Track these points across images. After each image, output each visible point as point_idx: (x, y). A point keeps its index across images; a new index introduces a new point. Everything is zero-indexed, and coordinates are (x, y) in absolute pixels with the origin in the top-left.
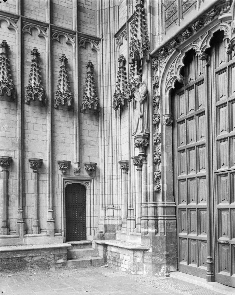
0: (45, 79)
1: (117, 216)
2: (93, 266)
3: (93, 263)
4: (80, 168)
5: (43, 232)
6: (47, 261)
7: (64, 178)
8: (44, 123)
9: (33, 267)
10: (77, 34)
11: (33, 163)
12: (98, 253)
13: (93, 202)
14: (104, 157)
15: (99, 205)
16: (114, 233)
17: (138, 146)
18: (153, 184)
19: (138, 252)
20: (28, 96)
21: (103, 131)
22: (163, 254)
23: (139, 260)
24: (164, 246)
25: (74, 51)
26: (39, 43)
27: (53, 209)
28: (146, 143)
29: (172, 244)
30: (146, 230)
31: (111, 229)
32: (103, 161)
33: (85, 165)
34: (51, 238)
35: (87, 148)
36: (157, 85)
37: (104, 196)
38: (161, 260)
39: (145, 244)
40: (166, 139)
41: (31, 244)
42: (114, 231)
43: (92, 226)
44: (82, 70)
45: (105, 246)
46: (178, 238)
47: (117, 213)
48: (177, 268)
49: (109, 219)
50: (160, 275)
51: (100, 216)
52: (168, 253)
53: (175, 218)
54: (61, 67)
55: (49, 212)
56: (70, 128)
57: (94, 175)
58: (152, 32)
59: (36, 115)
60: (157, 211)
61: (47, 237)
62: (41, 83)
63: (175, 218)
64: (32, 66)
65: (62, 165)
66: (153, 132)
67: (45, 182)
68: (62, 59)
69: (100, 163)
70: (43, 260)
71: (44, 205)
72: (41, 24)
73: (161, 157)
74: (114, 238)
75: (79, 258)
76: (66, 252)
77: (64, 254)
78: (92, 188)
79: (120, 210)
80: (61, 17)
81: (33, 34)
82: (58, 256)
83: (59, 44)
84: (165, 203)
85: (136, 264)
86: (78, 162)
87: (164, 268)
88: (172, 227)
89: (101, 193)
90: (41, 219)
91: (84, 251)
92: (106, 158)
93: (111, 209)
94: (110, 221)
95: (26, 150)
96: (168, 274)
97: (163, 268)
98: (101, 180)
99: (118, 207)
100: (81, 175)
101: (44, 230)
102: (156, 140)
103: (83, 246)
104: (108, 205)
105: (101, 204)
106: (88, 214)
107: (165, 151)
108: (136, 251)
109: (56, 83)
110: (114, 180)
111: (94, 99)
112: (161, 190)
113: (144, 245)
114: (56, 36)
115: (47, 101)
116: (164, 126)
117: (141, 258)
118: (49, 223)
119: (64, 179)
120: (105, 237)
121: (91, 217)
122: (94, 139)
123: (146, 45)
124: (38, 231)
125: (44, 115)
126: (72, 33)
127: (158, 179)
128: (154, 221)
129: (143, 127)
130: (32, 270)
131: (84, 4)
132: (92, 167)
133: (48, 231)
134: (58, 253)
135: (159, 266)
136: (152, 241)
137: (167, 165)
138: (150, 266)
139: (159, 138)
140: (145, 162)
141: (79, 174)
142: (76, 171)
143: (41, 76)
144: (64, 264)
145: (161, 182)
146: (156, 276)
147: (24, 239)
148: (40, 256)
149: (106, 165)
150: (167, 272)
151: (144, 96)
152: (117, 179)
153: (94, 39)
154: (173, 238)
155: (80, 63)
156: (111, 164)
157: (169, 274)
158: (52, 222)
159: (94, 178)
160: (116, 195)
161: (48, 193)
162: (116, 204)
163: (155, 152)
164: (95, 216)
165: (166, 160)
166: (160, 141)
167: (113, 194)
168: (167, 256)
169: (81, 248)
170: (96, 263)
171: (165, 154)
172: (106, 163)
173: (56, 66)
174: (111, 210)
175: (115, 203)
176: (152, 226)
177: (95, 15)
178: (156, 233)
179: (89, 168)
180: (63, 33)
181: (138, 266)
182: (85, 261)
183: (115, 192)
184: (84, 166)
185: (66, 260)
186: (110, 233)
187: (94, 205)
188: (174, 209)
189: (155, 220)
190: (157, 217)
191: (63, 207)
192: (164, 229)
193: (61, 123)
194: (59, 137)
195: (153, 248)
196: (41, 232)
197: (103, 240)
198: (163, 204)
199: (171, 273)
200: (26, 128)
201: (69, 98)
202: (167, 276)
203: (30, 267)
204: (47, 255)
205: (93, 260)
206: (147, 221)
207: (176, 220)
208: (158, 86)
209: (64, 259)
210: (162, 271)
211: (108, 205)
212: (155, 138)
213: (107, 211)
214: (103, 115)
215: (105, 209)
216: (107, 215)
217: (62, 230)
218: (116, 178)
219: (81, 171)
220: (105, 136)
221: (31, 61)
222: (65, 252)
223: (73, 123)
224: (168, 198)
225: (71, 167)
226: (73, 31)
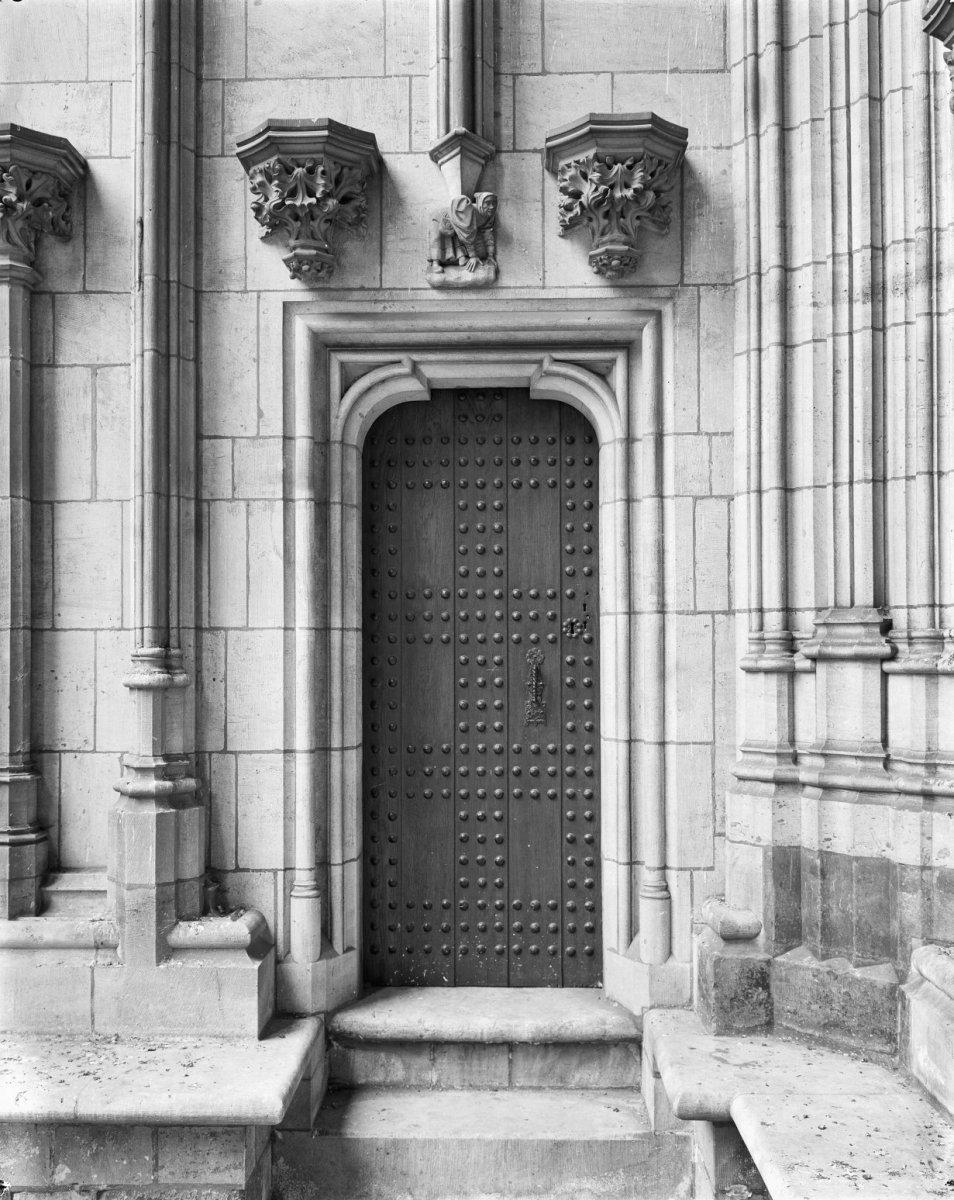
4: (494, 201)
5: (72, 903)
7: (320, 324)
14: (783, 47)
15: (730, 612)
16: (881, 975)
31: (847, 916)
37: (772, 500)
42: (887, 947)
43: (648, 854)
49: (828, 789)
51: (740, 741)
55: (133, 688)
57: (662, 276)
61: (81, 960)
69: (738, 135)
71: (107, 617)
78: (644, 427)
89: (741, 479)
90: (67, 758)
93: (853, 673)
94: (841, 810)
100: (505, 281)
103: (538, 1065)
104: (819, 610)
105: (743, 599)
110: (895, 306)
119: (324, 347)
120: (784, 1004)
121: (631, 742)
132: (617, 167)
141: (483, 273)
142: (448, 239)
149: (801, 141)
156: (860, 111)
159: (667, 309)
160: (920, 485)
162: (921, 596)
164: (671, 736)
167: (879, 481)
169: (520, 1081)
172: (800, 110)
174: (858, 681)
175: (907, 590)
179: (588, 191)
187: (662, 610)
191: (303, 639)
196: (57, 900)
197: (751, 1031)
211: (825, 616)
213: (806, 686)
216: (806, 736)
217: (289, 886)
218: (917, 261)
219: (508, 240)
225: (399, 202)
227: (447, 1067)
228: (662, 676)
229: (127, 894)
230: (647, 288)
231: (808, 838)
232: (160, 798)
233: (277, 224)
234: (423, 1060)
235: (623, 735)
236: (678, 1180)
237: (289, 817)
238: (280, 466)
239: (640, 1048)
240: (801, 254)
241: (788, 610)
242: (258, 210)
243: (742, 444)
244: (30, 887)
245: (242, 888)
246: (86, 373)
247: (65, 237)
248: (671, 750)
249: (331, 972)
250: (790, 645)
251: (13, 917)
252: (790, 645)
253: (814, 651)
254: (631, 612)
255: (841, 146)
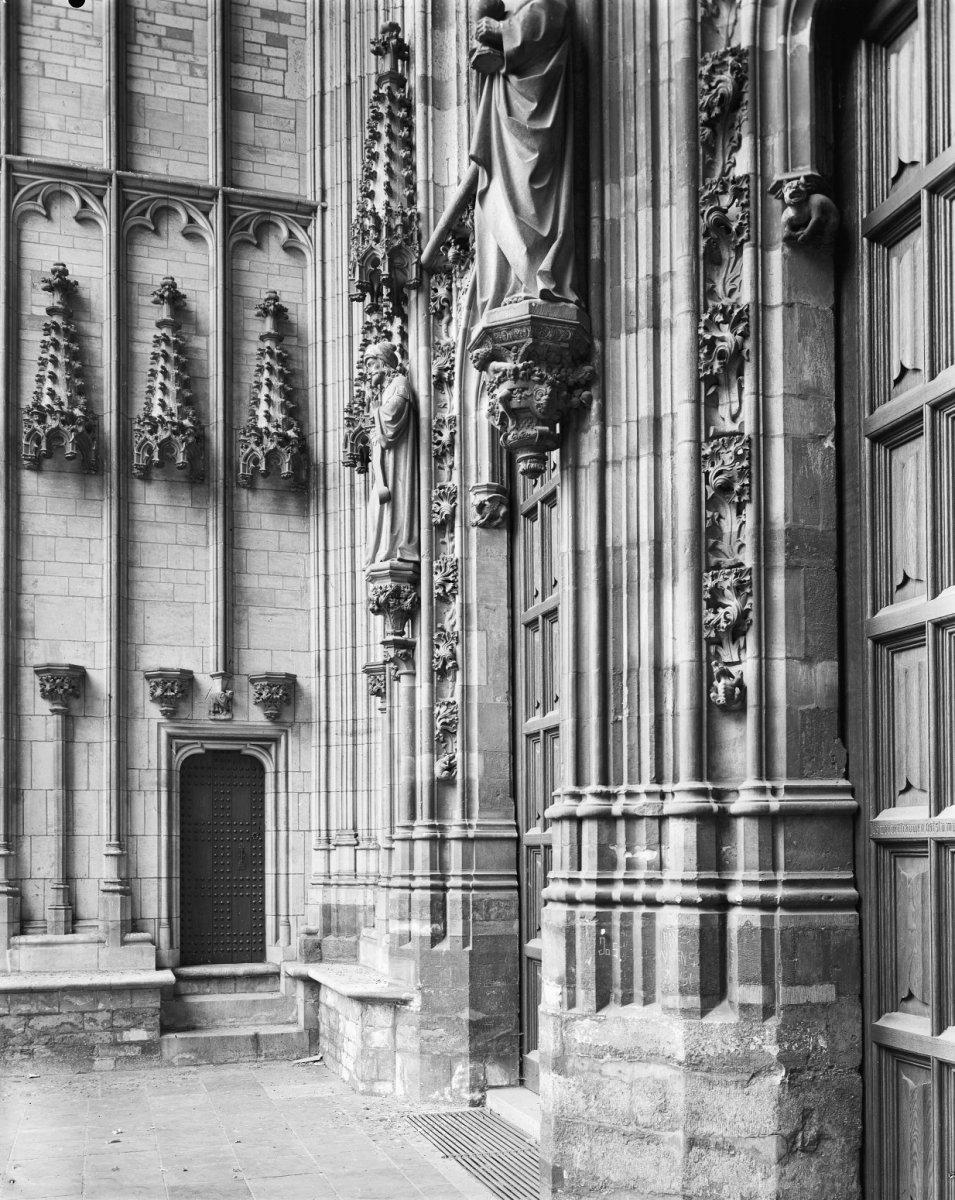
0: (99, 372)
1: (367, 872)
2: (262, 1058)
3: (263, 1046)
4: (232, 694)
5: (84, 930)
6: (86, 1032)
7: (170, 731)
8: (97, 535)
9: (31, 1053)
10: (220, 197)
11: (47, 680)
12: (294, 1013)
13: (285, 820)
14: (327, 650)
15: (310, 831)
16: (353, 939)
17: (380, 609)
18: (431, 751)
19: (377, 1008)
20: (27, 440)
21: (322, 553)
22: (458, 1019)
23: (380, 1038)
24: (465, 989)
25: (212, 262)
26: (78, 243)
27: (120, 846)
28: (406, 600)
29: (498, 983)
30: (405, 927)
32: (324, 666)
33: (252, 681)
34: (111, 951)
35: (262, 617)
36: (446, 375)
37: (323, 795)
38: (453, 1040)
39: (400, 979)
40: (478, 580)
41: (35, 972)
42: (355, 931)
43: (283, 911)
44: (246, 328)
45: (313, 985)
46: (525, 960)
47: (368, 861)
48: (521, 1073)
50: (449, 1097)
51: (313, 873)
52: (480, 1015)
53: (515, 883)
54: (160, 325)
55: (107, 855)
56: (193, 546)
57: (287, 718)
58: (430, 176)
59: (65, 507)
60: (446, 855)
61: (94, 947)
62: (81, 391)
63: (515, 883)
64: (47, 329)
65: (157, 684)
66: (434, 553)
67: (97, 747)
68: (162, 296)
70: (68, 1028)
71: (93, 830)
72: (84, 176)
73: (458, 649)
74: (352, 955)
75: (218, 1027)
76: (158, 1004)
77: (150, 1012)
78: (282, 768)
79: (378, 849)
80: (161, 140)
81: (56, 212)
82: (126, 1017)
83: (155, 241)
84: (470, 826)
85: (371, 1054)
86: (221, 671)
87: (462, 1070)
88: (498, 916)
89: (313, 788)
91: (240, 1003)
92: (332, 654)
93: (348, 848)
94: (343, 891)
95: (27, 634)
96: (477, 1096)
97: (460, 1074)
98: (315, 738)
99: (370, 839)
101: (89, 923)
102: (443, 585)
103: (245, 984)
105: (314, 826)
106: (269, 868)
107: (474, 626)
108: (370, 1007)
109: (141, 388)
110: (359, 738)
111: (279, 435)
112: (459, 777)
113: (396, 982)
114: (143, 213)
115: (103, 452)
116: (474, 531)
117: (388, 1031)
118: (106, 895)
119: (171, 737)
122: (290, 582)
123: (406, 227)
124: (62, 925)
125: (95, 506)
126: (202, 194)
127: (447, 731)
128: (429, 893)
129: (394, 540)
130: (28, 1065)
131: (253, 80)
133: (101, 927)
134: (127, 1006)
135: (447, 1063)
136: (422, 970)
137: (484, 677)
138: (414, 1064)
139: (451, 578)
140: (404, 669)
141: (228, 717)
142: (217, 705)
143: (77, 365)
144: (148, 1049)
145: (458, 746)
146: (436, 1102)
147: (8, 952)
148: (59, 1013)
149: (332, 680)
150: (472, 1089)
151: (393, 421)
152: (369, 732)
153: (294, 207)
154: (503, 956)
155: (239, 303)
157: (484, 1097)
158: (114, 891)
159: (290, 730)
161: (105, 786)
163: (442, 629)
164: (291, 871)
165: (480, 660)
166: (454, 588)
167: (355, 791)
168: (475, 1027)
170: (278, 1047)
171: (475, 637)
172: (332, 672)
173: (143, 322)
174: (348, 851)
175: (362, 825)
176: (421, 912)
177: (299, 116)
178: (436, 938)
179: (264, 696)
180: (167, 199)
181: (377, 1062)
182: (231, 1038)
183: (362, 784)
184: (251, 686)
185: (155, 1034)
186: (342, 938)
187: (287, 830)
188: (512, 847)
189: (432, 888)
190: (444, 878)
191: (164, 839)
192: (466, 925)
193: (158, 530)
194: (150, 584)
195: (423, 995)
196: (78, 929)
197: (315, 962)
198: (465, 827)
199: (490, 1093)
200: (26, 553)
201: (178, 439)
202: (473, 1103)
203: (22, 1052)
204: (83, 1013)
205: (266, 1036)
206: (407, 892)
207: (519, 888)
208: (449, 377)
209: (148, 1030)
210: (455, 1084)
212: (438, 579)
213: (332, 853)
214: (322, 491)
215: (328, 844)
216: (333, 870)
217: (160, 924)
219: (236, 705)
220: (331, 571)
221: (43, 312)
222: (153, 1003)
223: (207, 527)
224: (488, 805)
226: (205, 189)
227: (213, 986)
228: (288, 852)
229: (110, 924)
230: (283, 723)
231: (333, 902)
232: (121, 892)
233: (158, 700)
234: (205, 985)
235: (274, 872)
236: (292, 1011)
237: (159, 901)
238: (156, 779)
239: (279, 976)
240: (333, 718)
241: (328, 830)
242: (152, 694)
243: (314, 776)
244: (70, 924)
245: (143, 924)
246: (85, 745)
247: (78, 697)
248: (291, 876)
249: (173, 954)
250: (328, 841)
251: (66, 934)
252: (328, 841)
253: (335, 843)
254: (277, 831)
255: (344, 686)
